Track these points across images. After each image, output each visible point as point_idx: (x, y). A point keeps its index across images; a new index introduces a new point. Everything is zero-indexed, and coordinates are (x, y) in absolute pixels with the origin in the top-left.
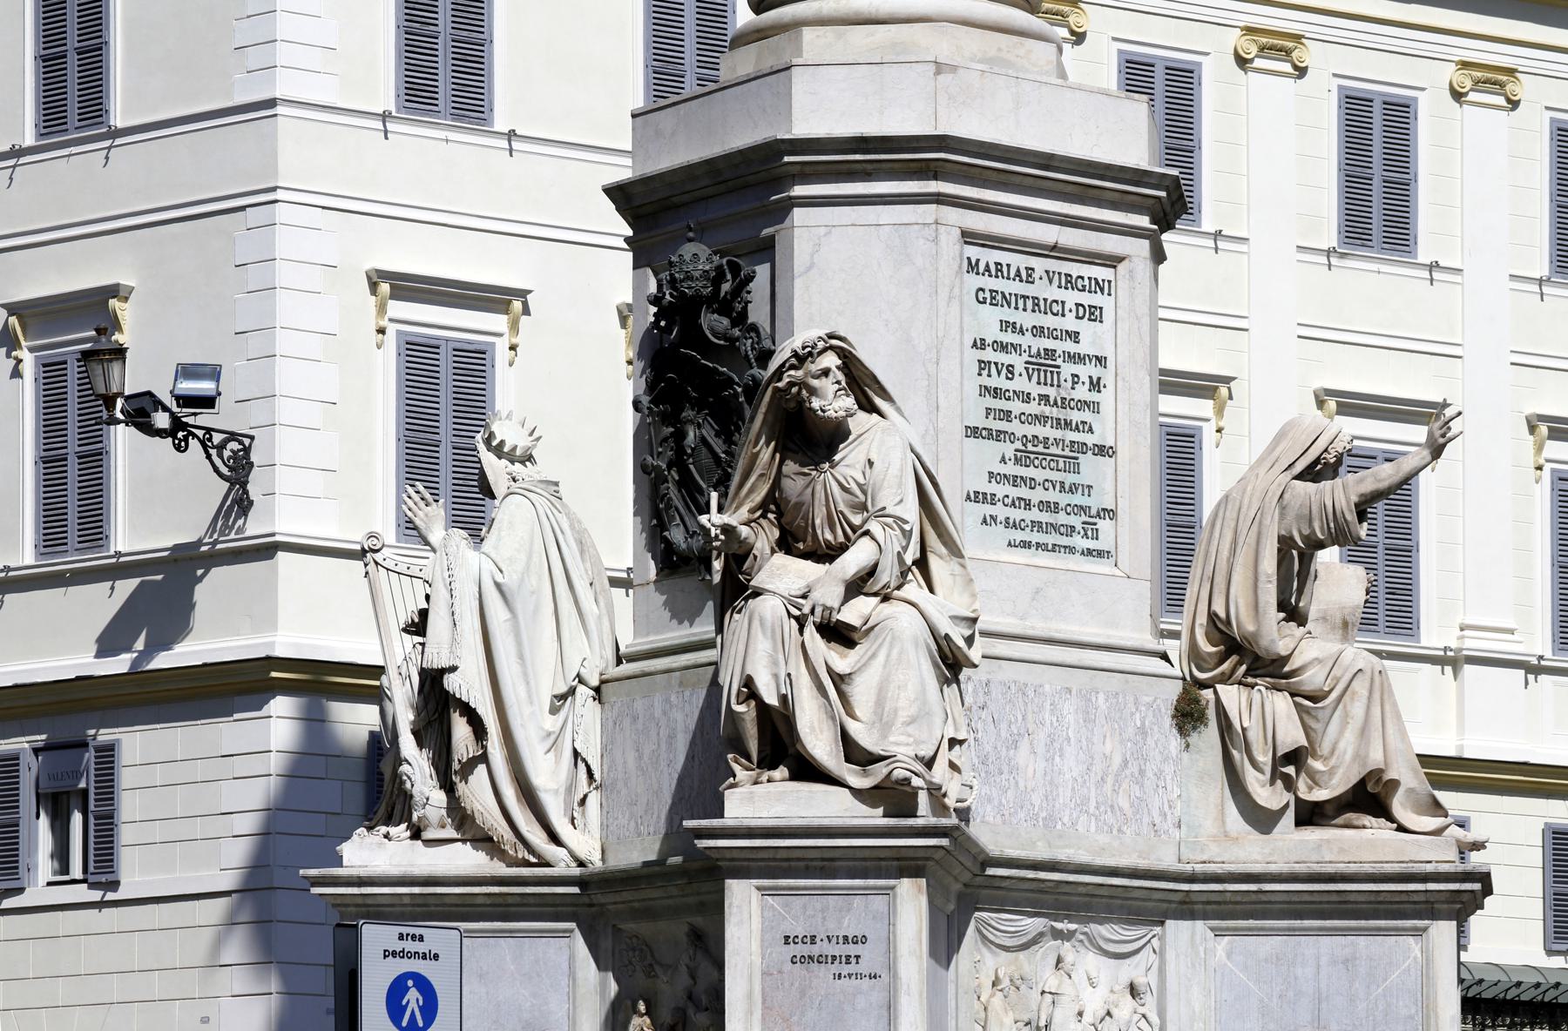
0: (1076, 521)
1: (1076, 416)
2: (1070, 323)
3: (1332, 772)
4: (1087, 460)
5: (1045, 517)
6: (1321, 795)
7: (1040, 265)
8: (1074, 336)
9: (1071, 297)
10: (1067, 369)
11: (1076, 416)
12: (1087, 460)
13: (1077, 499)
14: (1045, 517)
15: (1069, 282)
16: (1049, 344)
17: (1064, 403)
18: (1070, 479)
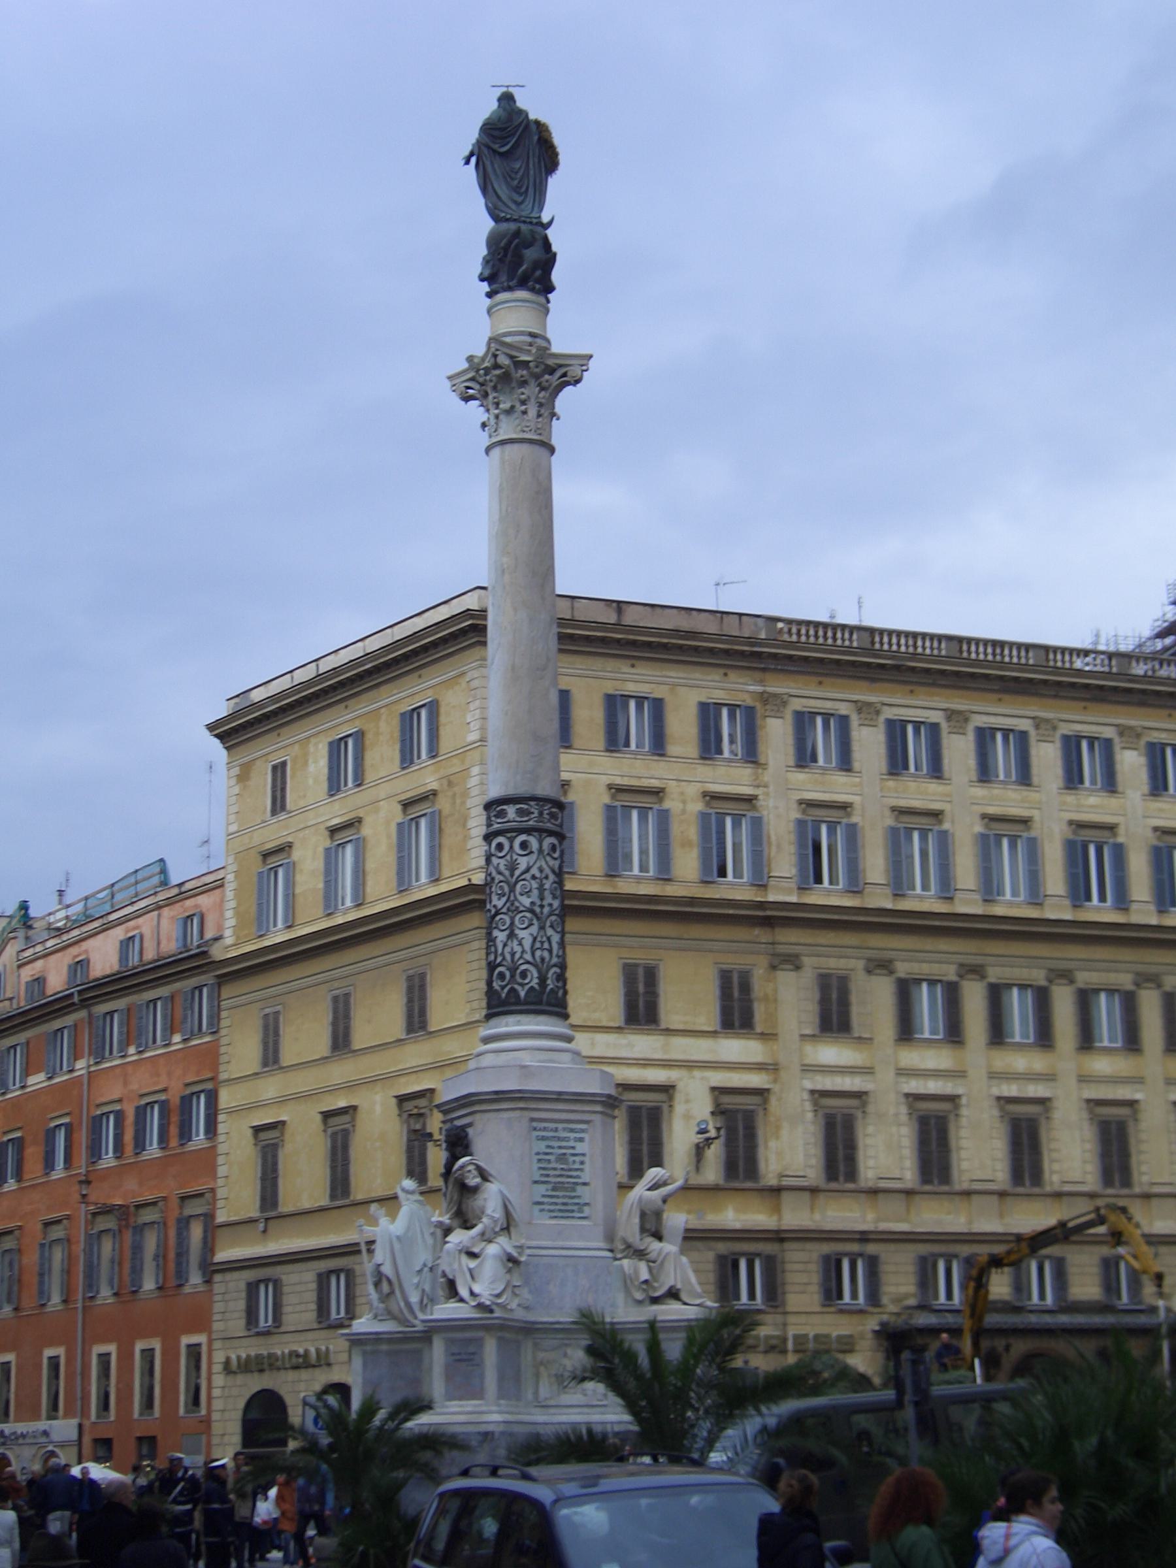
0: (575, 1208)
1: (574, 1173)
2: (571, 1144)
3: (660, 1287)
4: (579, 1188)
5: (563, 1208)
6: (657, 1294)
7: (560, 1126)
8: (573, 1148)
9: (572, 1135)
10: (572, 1159)
11: (574, 1173)
12: (579, 1188)
13: (576, 1201)
14: (563, 1208)
15: (572, 1130)
16: (564, 1151)
17: (570, 1170)
18: (573, 1194)
